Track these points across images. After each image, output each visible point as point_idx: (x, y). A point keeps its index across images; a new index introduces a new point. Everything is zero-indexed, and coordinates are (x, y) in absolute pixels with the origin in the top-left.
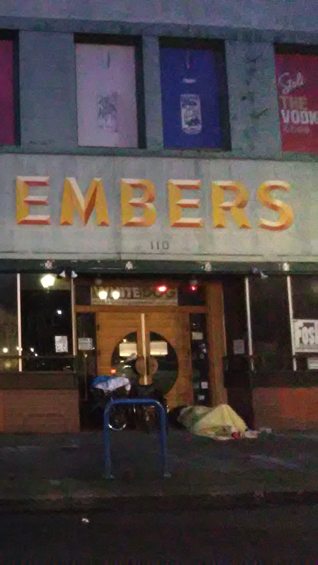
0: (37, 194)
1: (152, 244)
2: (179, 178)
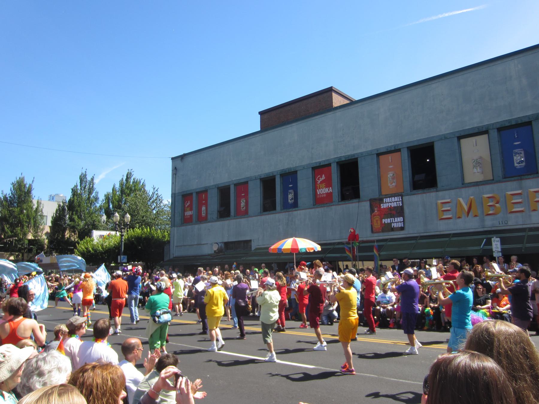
0: (446, 207)
1: (499, 222)
2: (511, 191)
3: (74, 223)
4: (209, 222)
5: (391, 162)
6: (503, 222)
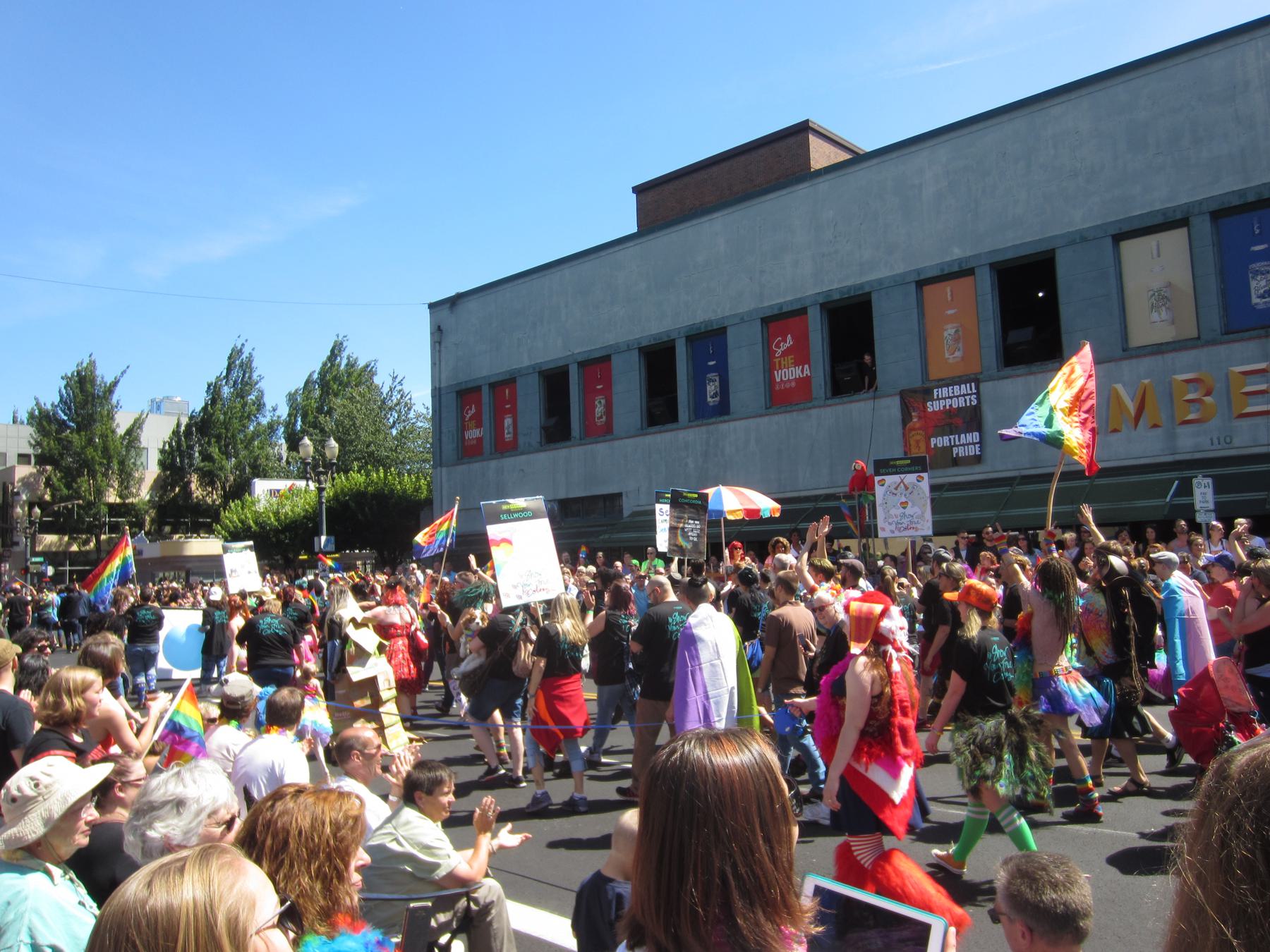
1: (1212, 440)
2: (1243, 364)
3: (211, 464)
4: (522, 453)
5: (952, 300)
6: (1222, 440)
